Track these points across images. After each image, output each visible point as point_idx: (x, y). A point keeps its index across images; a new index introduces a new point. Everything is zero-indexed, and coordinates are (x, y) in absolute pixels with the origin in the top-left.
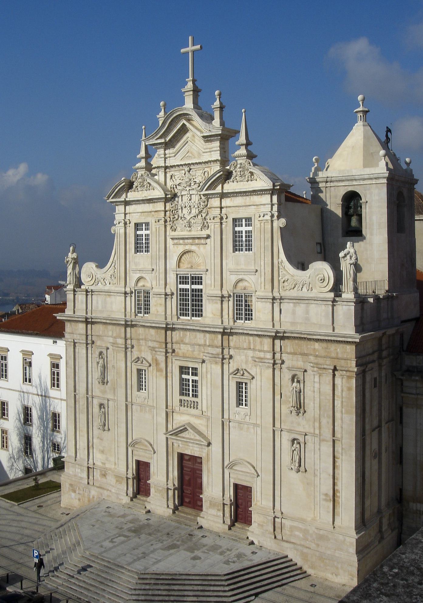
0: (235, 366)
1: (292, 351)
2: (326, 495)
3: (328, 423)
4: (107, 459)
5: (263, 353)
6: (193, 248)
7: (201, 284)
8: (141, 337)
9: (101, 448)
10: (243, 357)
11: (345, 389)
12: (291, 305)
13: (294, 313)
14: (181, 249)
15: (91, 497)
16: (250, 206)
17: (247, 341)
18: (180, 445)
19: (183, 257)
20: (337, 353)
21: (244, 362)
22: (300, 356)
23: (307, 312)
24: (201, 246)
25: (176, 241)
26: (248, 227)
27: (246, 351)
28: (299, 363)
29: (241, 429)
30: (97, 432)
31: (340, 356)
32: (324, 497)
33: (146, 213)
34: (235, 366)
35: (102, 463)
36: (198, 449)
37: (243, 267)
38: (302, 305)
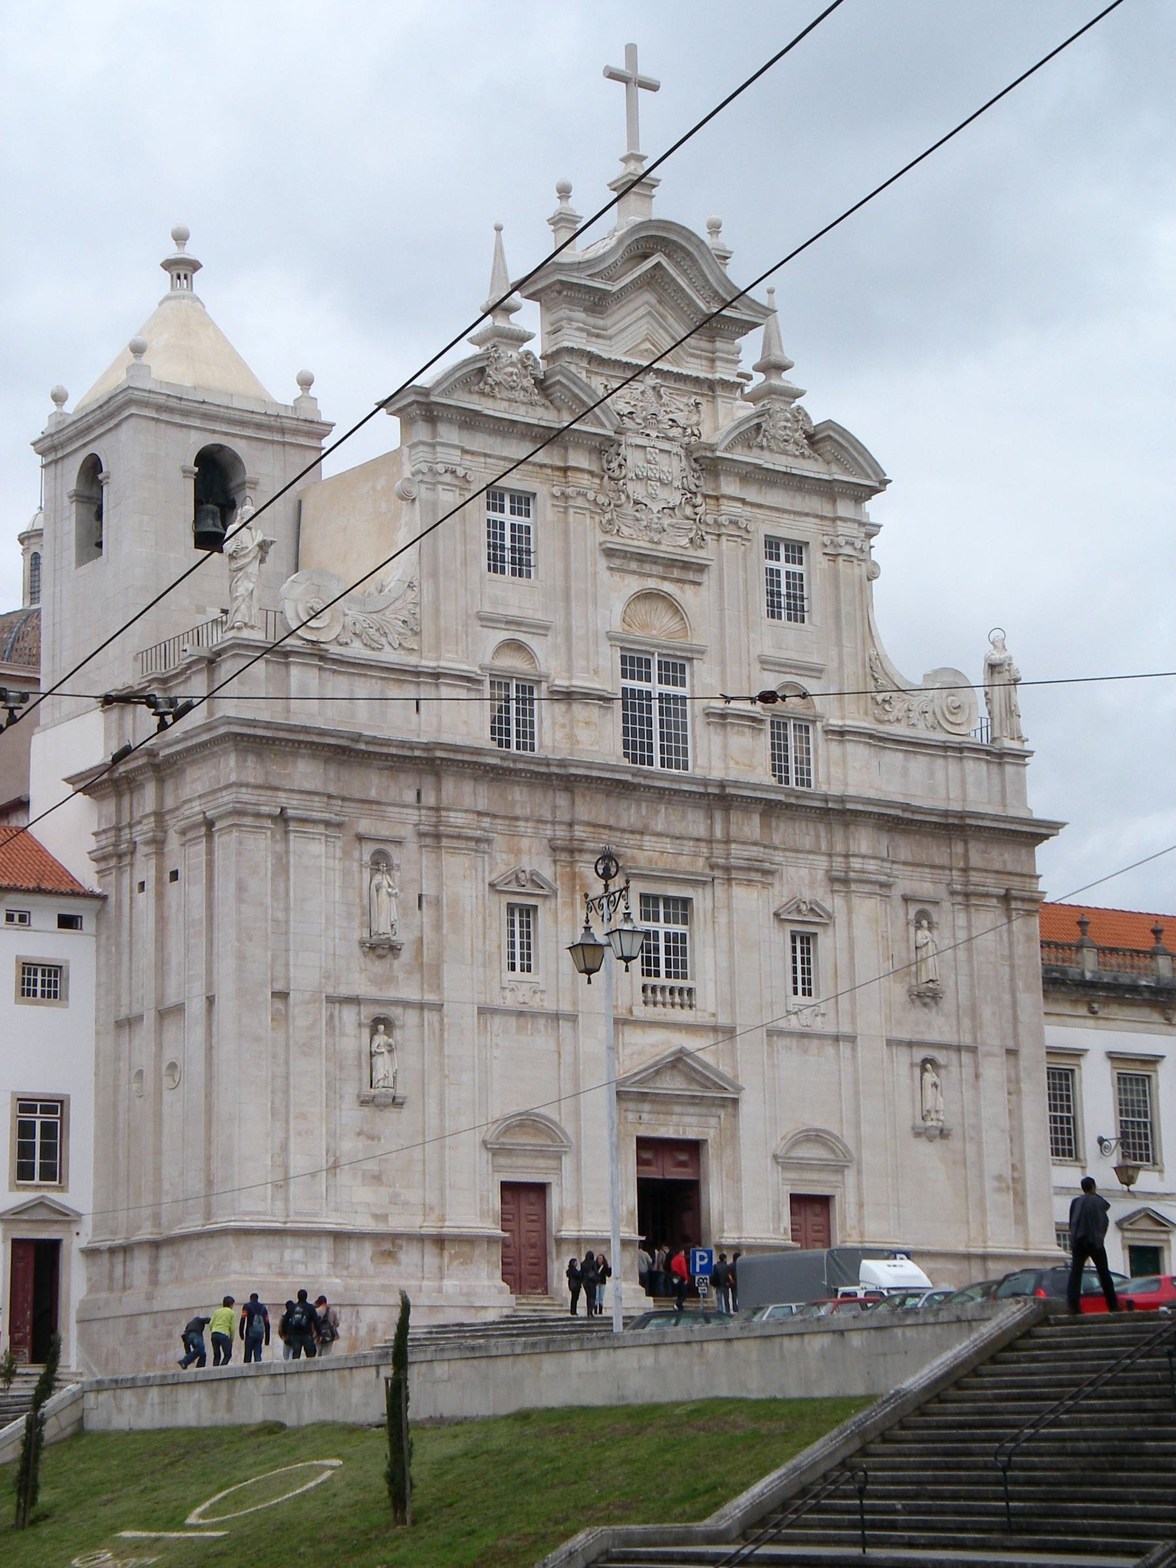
0: (785, 893)
1: (910, 859)
2: (999, 1178)
3: (994, 1014)
4: (394, 1200)
5: (859, 860)
6: (667, 587)
7: (683, 685)
8: (518, 812)
9: (372, 1166)
10: (804, 872)
11: (1022, 939)
12: (900, 755)
13: (905, 773)
14: (635, 585)
15: (363, 1331)
16: (807, 515)
17: (812, 833)
18: (645, 1116)
20: (1004, 862)
21: (807, 882)
22: (927, 870)
23: (932, 775)
24: (687, 587)
25: (617, 563)
26: (791, 565)
27: (811, 857)
28: (924, 885)
29: (806, 1051)
30: (351, 1114)
31: (1010, 868)
32: (996, 1184)
34: (785, 893)
35: (376, 1217)
36: (693, 1120)
37: (793, 655)
38: (920, 758)
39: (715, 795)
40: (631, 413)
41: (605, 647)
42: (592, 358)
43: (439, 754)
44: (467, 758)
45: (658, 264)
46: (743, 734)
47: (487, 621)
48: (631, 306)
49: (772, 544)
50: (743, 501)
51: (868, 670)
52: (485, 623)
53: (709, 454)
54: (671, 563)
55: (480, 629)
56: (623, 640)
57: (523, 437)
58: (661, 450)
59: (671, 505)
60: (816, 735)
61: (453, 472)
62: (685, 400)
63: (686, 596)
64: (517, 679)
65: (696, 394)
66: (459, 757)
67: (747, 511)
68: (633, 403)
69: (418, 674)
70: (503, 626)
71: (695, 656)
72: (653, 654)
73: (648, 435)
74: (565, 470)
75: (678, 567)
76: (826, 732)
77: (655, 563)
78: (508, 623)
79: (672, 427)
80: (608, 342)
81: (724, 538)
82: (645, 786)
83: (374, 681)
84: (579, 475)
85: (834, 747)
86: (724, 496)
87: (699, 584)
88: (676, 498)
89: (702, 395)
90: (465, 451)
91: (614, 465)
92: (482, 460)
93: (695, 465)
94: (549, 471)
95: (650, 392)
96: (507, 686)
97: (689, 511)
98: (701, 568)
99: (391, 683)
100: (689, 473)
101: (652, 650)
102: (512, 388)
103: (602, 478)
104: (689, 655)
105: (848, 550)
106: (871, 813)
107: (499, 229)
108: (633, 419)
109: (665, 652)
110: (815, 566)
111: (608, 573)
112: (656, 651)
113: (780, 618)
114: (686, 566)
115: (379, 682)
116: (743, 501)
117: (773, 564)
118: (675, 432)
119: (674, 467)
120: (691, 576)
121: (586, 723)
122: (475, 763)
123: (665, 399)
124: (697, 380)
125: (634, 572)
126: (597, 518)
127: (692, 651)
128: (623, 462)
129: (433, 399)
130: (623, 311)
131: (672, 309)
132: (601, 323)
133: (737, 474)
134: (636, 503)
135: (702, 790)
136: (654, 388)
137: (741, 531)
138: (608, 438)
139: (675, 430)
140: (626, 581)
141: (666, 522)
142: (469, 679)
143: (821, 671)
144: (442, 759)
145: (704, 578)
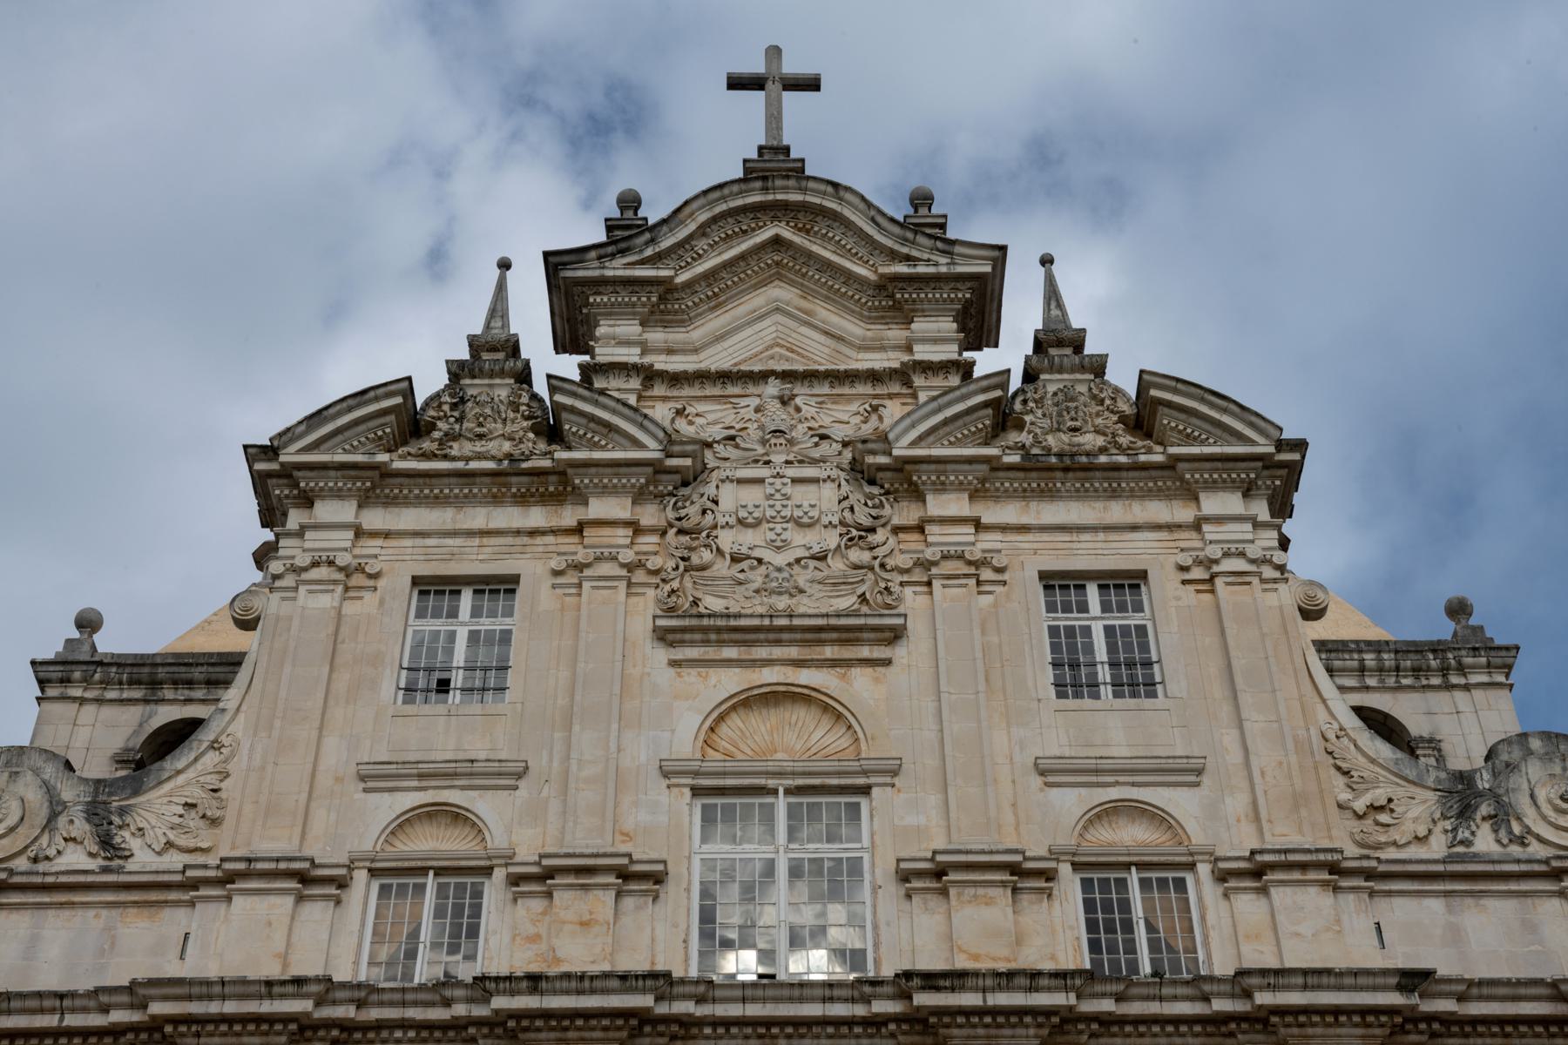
6: (806, 677)
12: (1436, 905)
13: (1455, 936)
14: (730, 682)
16: (1134, 528)
19: (724, 729)
23: (1530, 927)
33: (509, 540)
37: (1125, 752)
38: (1491, 903)
39: (897, 1019)
40: (732, 438)
41: (658, 791)
42: (650, 376)
43: (157, 1008)
44: (230, 1007)
45: (777, 241)
46: (989, 902)
47: (375, 778)
48: (742, 310)
49: (1061, 585)
50: (978, 525)
51: (1321, 756)
52: (370, 784)
53: (883, 460)
54: (815, 634)
55: (363, 795)
56: (696, 774)
57: (496, 500)
58: (795, 481)
59: (816, 549)
60: (1202, 886)
61: (331, 563)
62: (854, 407)
63: (858, 688)
64: (439, 872)
65: (876, 396)
66: (214, 1008)
67: (989, 541)
68: (738, 426)
69: (194, 884)
70: (415, 783)
71: (872, 780)
72: (775, 792)
73: (767, 463)
74: (579, 529)
75: (833, 642)
76: (1222, 877)
77: (778, 642)
78: (421, 776)
79: (816, 445)
80: (694, 358)
81: (936, 584)
82: (716, 1022)
83: (91, 913)
84: (607, 531)
85: (1248, 905)
86: (932, 520)
87: (887, 662)
88: (832, 539)
89: (890, 396)
90: (359, 533)
91: (692, 510)
92: (408, 542)
93: (868, 489)
94: (550, 539)
95: (774, 406)
96: (420, 889)
97: (856, 555)
98: (895, 635)
99: (132, 911)
100: (856, 498)
101: (771, 783)
102: (481, 436)
103: (664, 533)
104: (861, 781)
105: (1239, 565)
106: (1337, 1011)
107: (505, 265)
108: (737, 446)
109: (800, 782)
110: (1170, 611)
111: (672, 671)
112: (781, 784)
113: (1097, 696)
114: (849, 635)
115: (104, 912)
116: (978, 525)
117: (1075, 620)
118: (826, 449)
119: (825, 500)
120: (865, 652)
121: (582, 924)
122: (258, 1019)
123: (808, 411)
124: (874, 377)
125: (728, 663)
126: (651, 593)
127: (865, 773)
128: (709, 505)
129: (282, 458)
130: (727, 317)
131: (827, 299)
132: (676, 336)
133: (960, 487)
134: (736, 559)
135: (860, 1010)
136: (784, 401)
137: (980, 571)
138: (658, 469)
139: (825, 445)
140: (713, 680)
141: (802, 577)
142: (307, 879)
143: (1199, 772)
144: (176, 1020)
145: (899, 653)
